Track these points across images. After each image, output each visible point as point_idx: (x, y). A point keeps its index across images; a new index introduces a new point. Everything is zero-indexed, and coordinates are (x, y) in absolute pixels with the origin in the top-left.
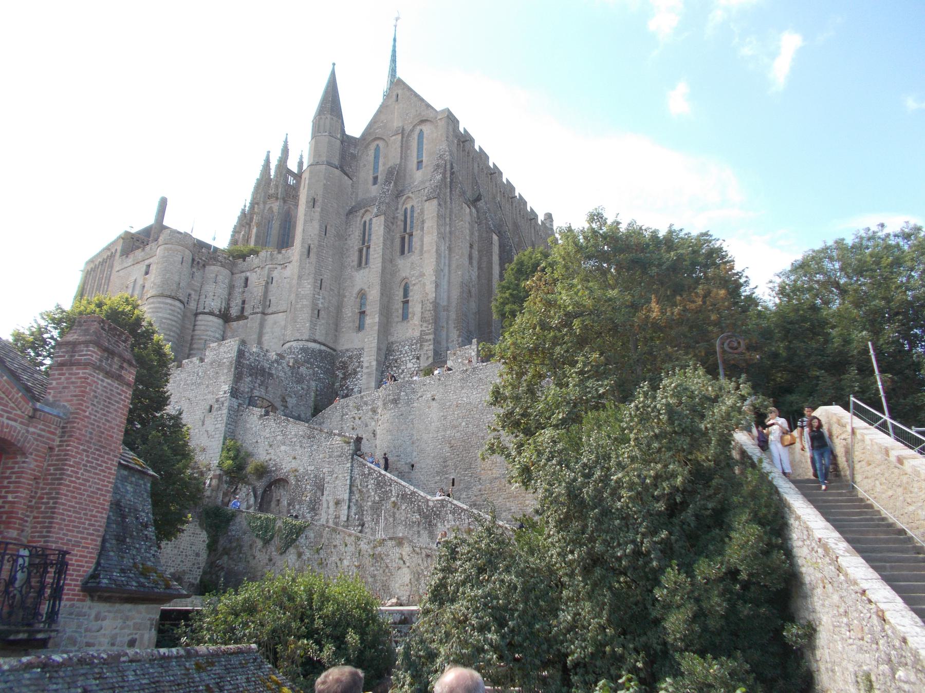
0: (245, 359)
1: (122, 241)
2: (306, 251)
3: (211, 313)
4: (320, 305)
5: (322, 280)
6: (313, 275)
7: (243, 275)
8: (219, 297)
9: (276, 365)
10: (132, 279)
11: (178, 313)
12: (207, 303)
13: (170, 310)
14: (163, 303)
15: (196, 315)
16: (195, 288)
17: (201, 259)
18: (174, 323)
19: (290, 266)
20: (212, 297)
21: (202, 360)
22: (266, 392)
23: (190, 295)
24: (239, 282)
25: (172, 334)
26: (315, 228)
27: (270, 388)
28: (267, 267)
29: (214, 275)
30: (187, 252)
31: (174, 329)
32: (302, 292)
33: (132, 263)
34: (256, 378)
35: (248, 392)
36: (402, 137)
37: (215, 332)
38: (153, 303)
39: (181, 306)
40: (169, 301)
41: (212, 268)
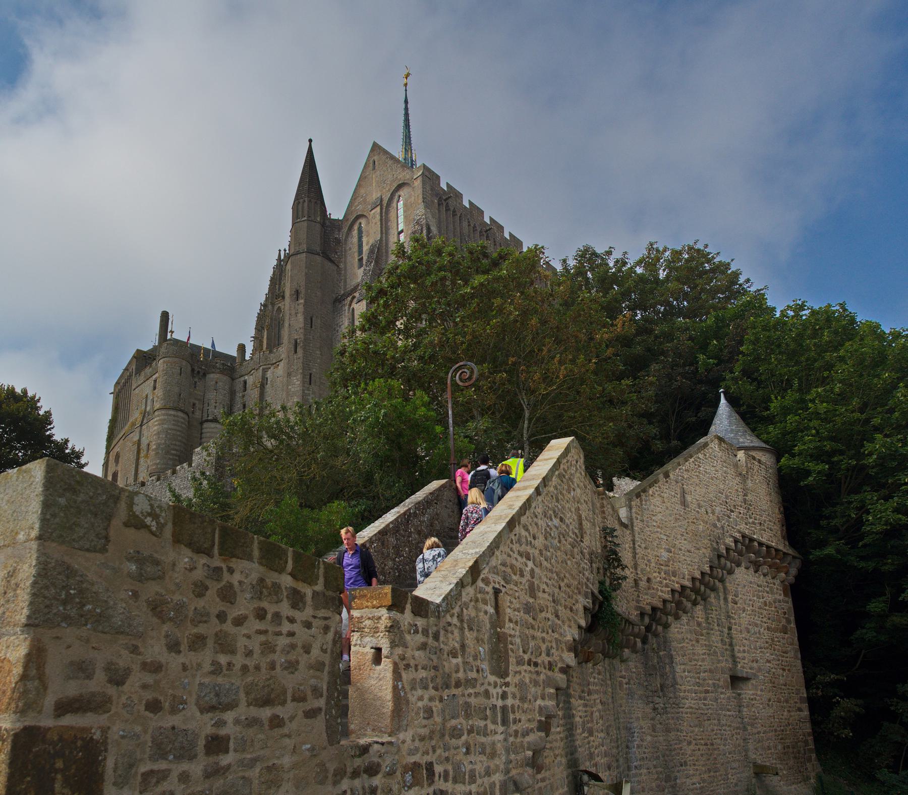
1: (135, 360)
2: (292, 347)
5: (311, 374)
6: (301, 371)
7: (242, 379)
8: (220, 403)
10: (144, 395)
11: (182, 423)
12: (210, 410)
14: (167, 415)
15: (202, 423)
17: (201, 368)
18: (178, 433)
19: (282, 364)
21: (190, 465)
23: (194, 404)
24: (239, 386)
25: (178, 443)
26: (299, 321)
28: (261, 368)
30: (184, 363)
31: (179, 438)
32: (293, 390)
33: (145, 379)
36: (381, 209)
38: (158, 416)
39: (186, 417)
40: (172, 412)
41: (212, 376)
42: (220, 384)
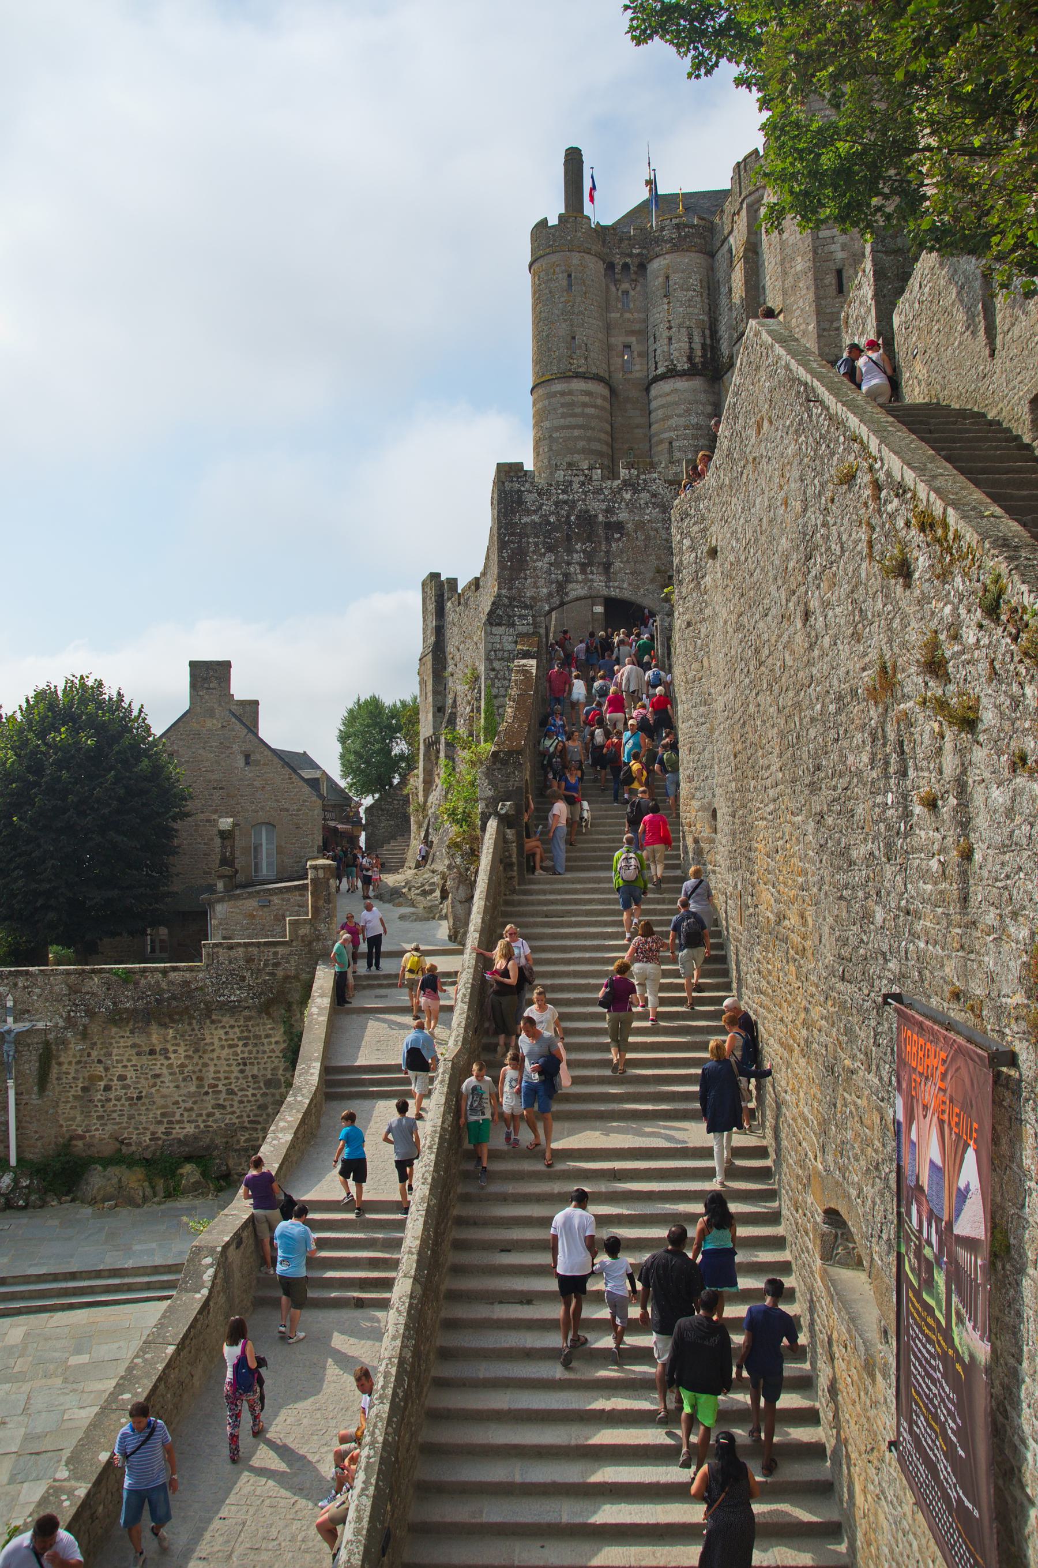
0: (528, 512)
3: (672, 373)
4: (840, 255)
7: (726, 247)
8: (680, 326)
9: (627, 496)
13: (563, 405)
16: (637, 327)
20: (666, 334)
22: (609, 580)
27: (618, 565)
29: (661, 279)
34: (570, 551)
35: (550, 595)
37: (688, 411)
40: (558, 387)
42: (675, 278)
